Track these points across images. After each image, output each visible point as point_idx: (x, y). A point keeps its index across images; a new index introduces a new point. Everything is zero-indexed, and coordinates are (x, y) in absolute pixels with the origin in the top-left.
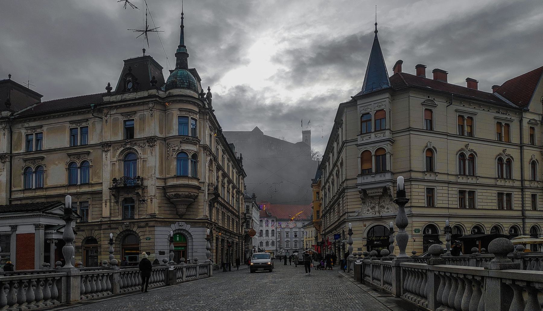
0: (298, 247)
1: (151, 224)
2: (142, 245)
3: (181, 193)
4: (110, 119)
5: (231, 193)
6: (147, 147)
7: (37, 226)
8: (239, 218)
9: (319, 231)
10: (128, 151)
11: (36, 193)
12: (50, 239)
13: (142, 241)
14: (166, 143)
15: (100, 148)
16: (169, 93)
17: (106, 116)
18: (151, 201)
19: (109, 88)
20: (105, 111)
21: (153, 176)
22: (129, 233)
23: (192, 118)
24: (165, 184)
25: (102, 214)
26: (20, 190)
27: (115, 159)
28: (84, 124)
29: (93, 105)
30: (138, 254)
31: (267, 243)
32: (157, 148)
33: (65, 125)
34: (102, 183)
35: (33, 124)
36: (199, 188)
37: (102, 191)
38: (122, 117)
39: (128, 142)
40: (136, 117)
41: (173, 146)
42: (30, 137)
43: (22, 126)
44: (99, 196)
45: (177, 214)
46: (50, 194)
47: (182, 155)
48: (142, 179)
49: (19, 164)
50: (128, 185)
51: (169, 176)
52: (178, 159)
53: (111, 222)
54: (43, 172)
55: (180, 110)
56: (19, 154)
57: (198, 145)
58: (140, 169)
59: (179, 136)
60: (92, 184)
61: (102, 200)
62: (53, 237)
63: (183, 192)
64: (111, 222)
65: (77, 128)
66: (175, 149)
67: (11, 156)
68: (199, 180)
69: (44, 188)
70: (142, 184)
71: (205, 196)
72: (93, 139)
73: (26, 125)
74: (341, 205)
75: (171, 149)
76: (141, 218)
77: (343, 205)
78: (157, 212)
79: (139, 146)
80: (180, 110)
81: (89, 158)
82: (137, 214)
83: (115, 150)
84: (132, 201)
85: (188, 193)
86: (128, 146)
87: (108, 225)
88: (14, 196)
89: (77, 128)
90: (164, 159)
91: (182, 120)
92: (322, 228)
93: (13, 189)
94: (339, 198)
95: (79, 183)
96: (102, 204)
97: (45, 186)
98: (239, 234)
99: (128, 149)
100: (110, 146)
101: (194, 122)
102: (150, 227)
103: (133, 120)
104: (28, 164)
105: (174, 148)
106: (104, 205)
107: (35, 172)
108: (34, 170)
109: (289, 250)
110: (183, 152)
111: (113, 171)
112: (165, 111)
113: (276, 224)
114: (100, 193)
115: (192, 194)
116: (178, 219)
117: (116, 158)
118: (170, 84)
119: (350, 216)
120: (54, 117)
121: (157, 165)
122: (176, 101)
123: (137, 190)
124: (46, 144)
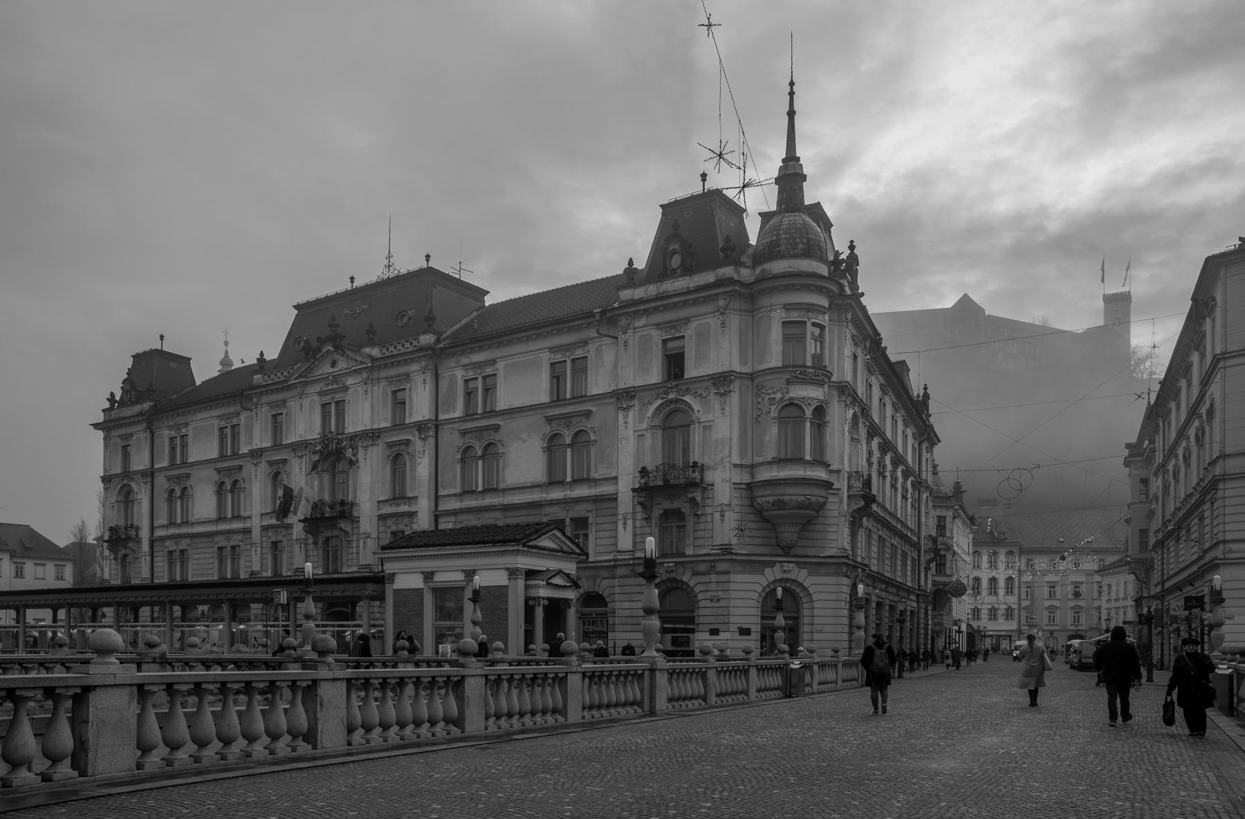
0: (1084, 623)
1: (722, 567)
2: (702, 612)
3: (789, 498)
4: (633, 338)
5: (900, 490)
6: (712, 396)
7: (513, 573)
8: (919, 551)
9: (1146, 584)
10: (671, 407)
11: (483, 499)
12: (534, 599)
13: (702, 604)
14: (755, 385)
15: (613, 403)
16: (763, 271)
17: (625, 333)
18: (722, 516)
19: (630, 270)
20: (623, 322)
21: (726, 460)
22: (674, 585)
23: (814, 324)
24: (753, 477)
25: (616, 544)
26: (455, 495)
27: (644, 426)
28: (579, 353)
29: (599, 310)
30: (693, 631)
31: (993, 613)
32: (735, 398)
33: (541, 355)
34: (616, 478)
35: (478, 357)
36: (828, 485)
37: (617, 494)
38: (659, 333)
39: (671, 388)
40: (690, 331)
41: (770, 391)
42: (471, 385)
43: (457, 362)
44: (611, 505)
45: (778, 546)
46: (511, 502)
47: (793, 412)
48: (702, 469)
49: (451, 440)
50: (672, 482)
51: (761, 460)
52: (782, 420)
53: (636, 562)
54: (497, 456)
55: (788, 307)
56: (451, 421)
57: (826, 386)
58: (697, 445)
59: (784, 367)
60: (596, 480)
61: (616, 515)
62: (541, 595)
63: (794, 495)
64: (636, 562)
65: (565, 361)
66: (774, 398)
67: (437, 425)
68: (829, 465)
69: (500, 490)
70: (702, 479)
71: (841, 502)
72: (598, 384)
73: (465, 360)
74: (1207, 521)
75: (767, 398)
76: (701, 553)
77: (1212, 522)
78: (734, 541)
79: (697, 395)
80: (788, 307)
81: (588, 425)
82: (691, 544)
83: (644, 406)
84: (678, 514)
85: (803, 498)
86: (672, 396)
87: (631, 568)
88: (446, 506)
89: (565, 361)
90: (751, 421)
91: (791, 330)
92: (1156, 577)
93: (442, 492)
94: (1200, 502)
95: (569, 479)
96: (616, 523)
97: (502, 486)
98: (919, 590)
99: (671, 401)
100: (634, 397)
101: (817, 331)
102: (719, 573)
103: (683, 337)
104: (469, 440)
105: (772, 396)
106: (620, 525)
107: (482, 457)
108: (480, 453)
109: (1057, 631)
110: (793, 403)
111: (639, 452)
112: (753, 311)
113: (1020, 563)
114: (613, 498)
115: (813, 499)
116: (781, 556)
117: (646, 423)
118: (764, 249)
119: (1230, 551)
120: (519, 341)
121: (736, 435)
122: (777, 287)
123: (692, 492)
124: (505, 398)
